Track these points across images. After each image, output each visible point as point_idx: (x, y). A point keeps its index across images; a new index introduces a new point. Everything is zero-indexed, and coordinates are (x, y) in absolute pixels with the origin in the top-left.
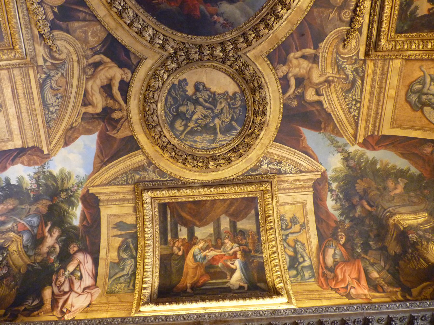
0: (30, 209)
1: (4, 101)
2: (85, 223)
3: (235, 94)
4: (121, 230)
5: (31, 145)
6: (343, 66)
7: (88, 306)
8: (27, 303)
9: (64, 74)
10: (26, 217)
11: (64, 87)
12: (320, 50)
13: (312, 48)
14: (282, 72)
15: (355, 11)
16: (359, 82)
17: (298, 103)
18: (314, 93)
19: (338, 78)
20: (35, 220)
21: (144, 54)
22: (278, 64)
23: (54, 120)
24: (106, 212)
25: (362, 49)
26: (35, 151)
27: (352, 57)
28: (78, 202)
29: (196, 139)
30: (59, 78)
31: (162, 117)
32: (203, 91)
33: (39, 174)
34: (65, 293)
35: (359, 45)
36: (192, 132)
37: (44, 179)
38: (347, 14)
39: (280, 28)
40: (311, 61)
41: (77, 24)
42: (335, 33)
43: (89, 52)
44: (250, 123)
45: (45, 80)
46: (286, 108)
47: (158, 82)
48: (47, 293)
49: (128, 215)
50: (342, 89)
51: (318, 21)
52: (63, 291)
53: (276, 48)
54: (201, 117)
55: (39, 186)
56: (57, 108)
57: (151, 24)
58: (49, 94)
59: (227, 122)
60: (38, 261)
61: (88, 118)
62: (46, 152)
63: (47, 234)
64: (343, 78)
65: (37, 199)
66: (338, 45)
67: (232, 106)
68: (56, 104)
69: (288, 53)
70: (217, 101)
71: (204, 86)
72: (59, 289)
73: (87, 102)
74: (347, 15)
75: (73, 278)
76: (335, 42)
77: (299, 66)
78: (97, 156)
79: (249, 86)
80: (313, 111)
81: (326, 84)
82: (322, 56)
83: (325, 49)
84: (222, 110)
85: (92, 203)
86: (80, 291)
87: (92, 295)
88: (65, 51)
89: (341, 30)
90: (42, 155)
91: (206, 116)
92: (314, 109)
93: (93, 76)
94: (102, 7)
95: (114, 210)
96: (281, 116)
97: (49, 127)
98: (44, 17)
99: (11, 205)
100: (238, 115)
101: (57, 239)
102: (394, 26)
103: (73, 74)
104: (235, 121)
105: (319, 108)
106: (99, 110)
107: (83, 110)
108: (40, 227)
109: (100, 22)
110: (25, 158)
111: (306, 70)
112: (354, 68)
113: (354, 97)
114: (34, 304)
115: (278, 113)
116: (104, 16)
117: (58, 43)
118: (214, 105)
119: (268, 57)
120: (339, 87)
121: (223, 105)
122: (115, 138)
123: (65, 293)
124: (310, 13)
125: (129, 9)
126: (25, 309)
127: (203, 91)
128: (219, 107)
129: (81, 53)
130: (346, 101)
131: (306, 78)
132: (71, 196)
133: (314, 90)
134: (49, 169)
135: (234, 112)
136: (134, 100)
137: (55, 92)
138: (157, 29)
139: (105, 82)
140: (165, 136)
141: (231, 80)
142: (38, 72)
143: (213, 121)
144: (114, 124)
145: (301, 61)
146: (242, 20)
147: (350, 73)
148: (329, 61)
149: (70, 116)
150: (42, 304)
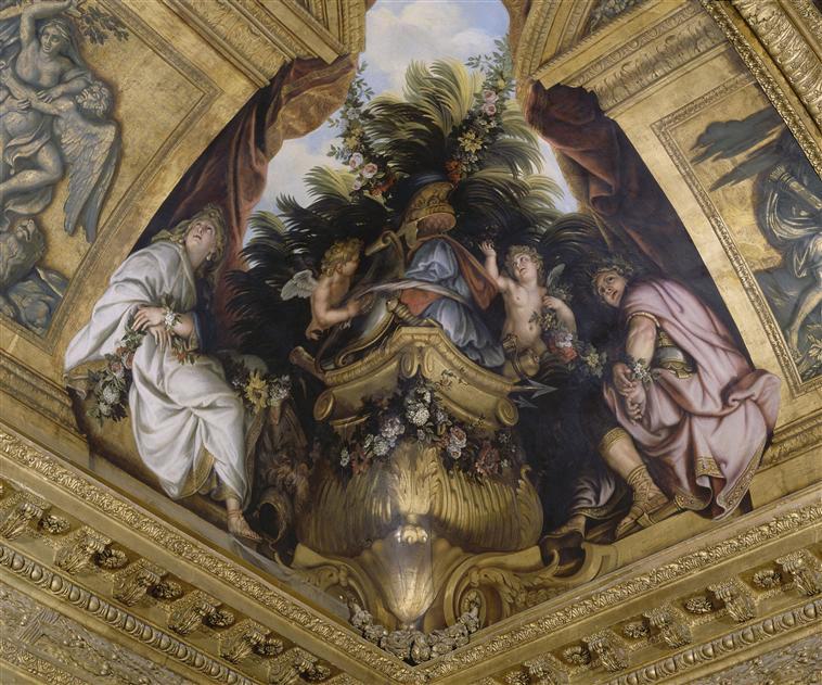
0: (403, 239)
2: (594, 192)
4: (730, 152)
5: (273, 70)
7: (769, 443)
8: (584, 504)
10: (408, 265)
20: (439, 260)
24: (639, 125)
26: (299, 74)
28: (531, 139)
34: (674, 431)
37: (382, 133)
48: (621, 452)
49: (726, 90)
52: (663, 427)
55: (382, 162)
60: (532, 373)
62: (329, 56)
63: (501, 283)
65: (403, 195)
72: (648, 427)
75: (670, 375)
85: (573, 115)
86: (713, 406)
87: (759, 405)
90: (326, 74)
95: (665, 98)
99: (344, 261)
101: (542, 283)
108: (468, 271)
110: (287, 114)
114: (603, 499)
123: (674, 431)
126: (591, 524)
132: (494, 132)
150: (625, 497)
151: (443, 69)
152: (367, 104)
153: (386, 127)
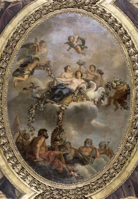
13: (135, 196)
21: (24, 191)
116: (3, 166)
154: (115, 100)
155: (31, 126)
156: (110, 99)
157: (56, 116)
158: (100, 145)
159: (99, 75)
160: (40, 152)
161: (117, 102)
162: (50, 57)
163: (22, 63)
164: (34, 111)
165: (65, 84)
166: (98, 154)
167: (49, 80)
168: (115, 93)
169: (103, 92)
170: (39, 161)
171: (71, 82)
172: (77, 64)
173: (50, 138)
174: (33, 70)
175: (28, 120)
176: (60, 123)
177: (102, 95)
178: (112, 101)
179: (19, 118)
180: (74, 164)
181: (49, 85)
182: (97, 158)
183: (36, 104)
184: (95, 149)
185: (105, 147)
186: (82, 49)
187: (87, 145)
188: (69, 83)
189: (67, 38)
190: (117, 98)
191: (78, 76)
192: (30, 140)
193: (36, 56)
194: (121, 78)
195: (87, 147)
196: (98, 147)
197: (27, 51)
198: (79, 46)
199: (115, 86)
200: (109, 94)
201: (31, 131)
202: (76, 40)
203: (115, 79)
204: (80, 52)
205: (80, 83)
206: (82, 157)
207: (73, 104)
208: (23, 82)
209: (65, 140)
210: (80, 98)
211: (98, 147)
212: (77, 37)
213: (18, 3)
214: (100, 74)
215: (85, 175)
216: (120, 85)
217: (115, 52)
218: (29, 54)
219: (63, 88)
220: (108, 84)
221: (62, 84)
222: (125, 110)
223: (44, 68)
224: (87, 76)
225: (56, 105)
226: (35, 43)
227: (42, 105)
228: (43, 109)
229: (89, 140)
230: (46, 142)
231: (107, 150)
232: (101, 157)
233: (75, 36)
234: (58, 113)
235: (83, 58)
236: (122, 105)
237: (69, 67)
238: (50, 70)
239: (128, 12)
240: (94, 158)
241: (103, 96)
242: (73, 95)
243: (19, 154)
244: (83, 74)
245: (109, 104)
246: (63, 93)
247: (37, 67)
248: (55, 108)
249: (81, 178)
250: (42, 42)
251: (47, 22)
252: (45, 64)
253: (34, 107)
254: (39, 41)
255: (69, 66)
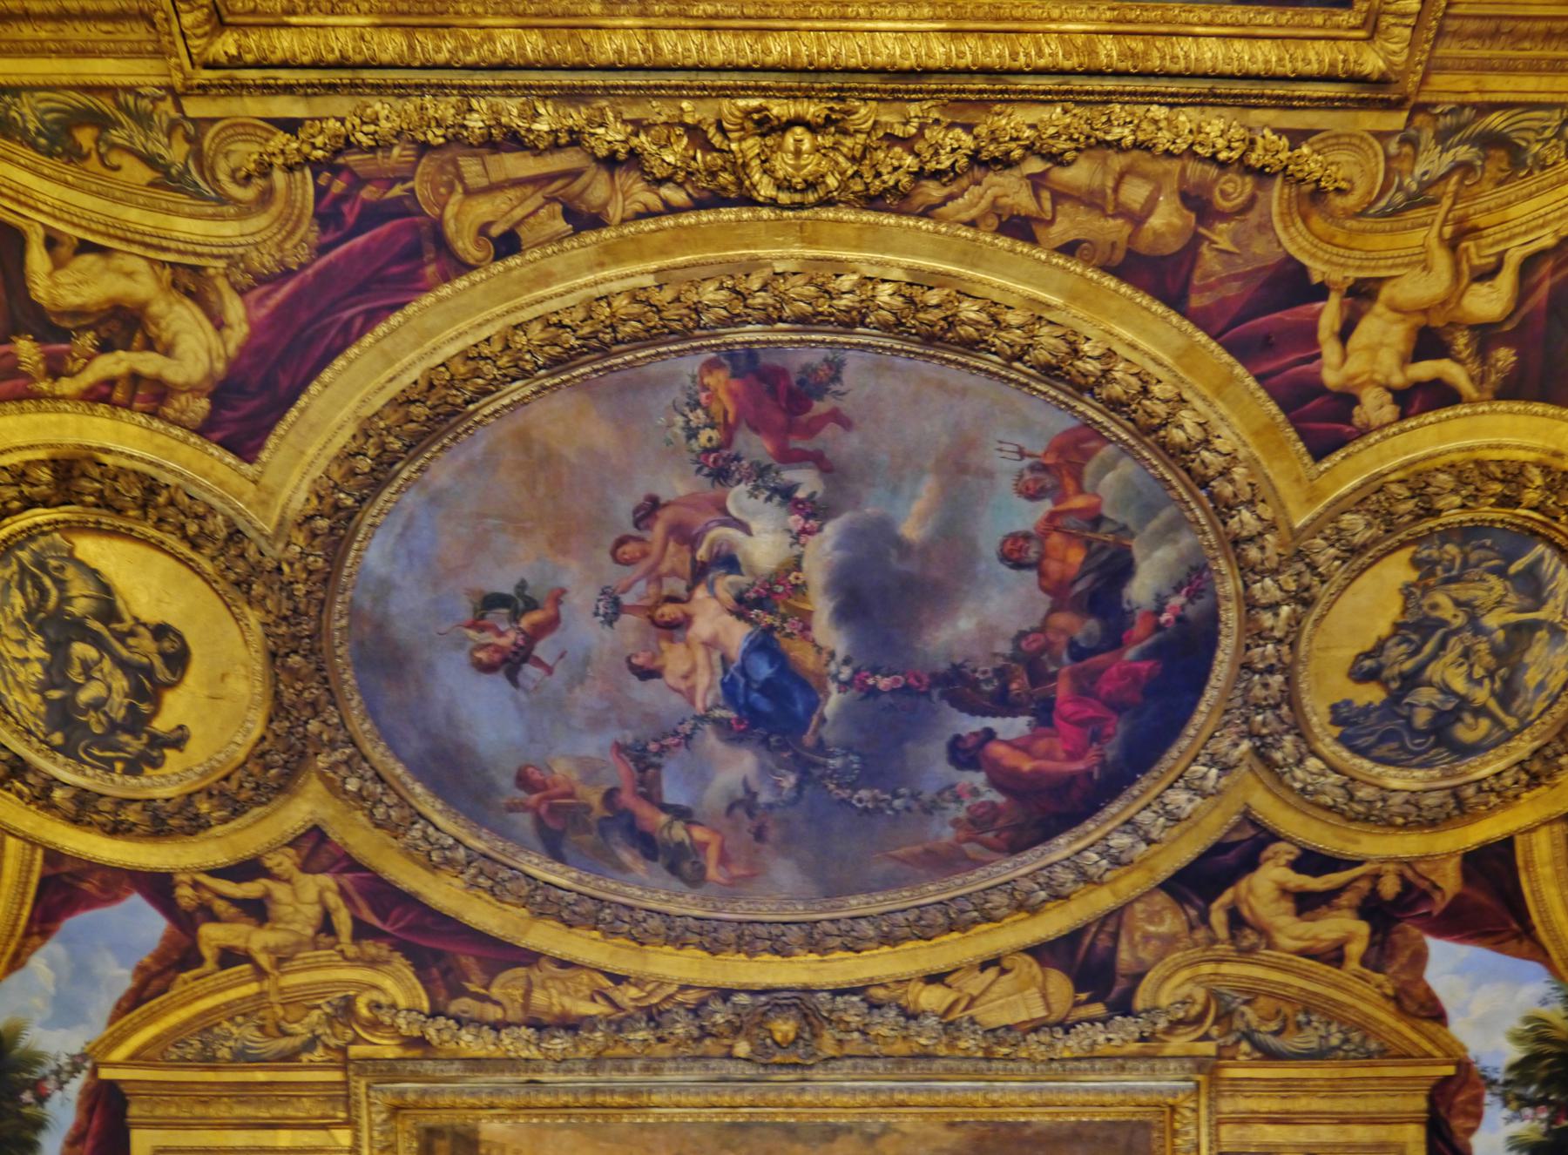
1: (1297, 1146)
3: (1415, 563)
6: (1414, 187)
9: (1246, 997)
11: (1281, 1003)
12: (1336, 276)
13: (1319, 305)
14: (1381, 407)
15: (1224, 165)
16: (1496, 121)
17: (1508, 345)
18: (1481, 289)
19: (1454, 203)
21: (1235, 809)
22: (1350, 424)
23: (1365, 1038)
25: (1371, 120)
27: (1388, 158)
29: (1532, 684)
30: (1256, 1010)
31: (1433, 779)
32: (1383, 660)
33: (1510, 1096)
35: (1350, 136)
36: (1506, 696)
37: (1527, 1085)
38: (1229, 188)
39: (1234, 420)
40: (1365, 306)
41: (1124, 956)
42: (1286, 228)
43: (1200, 934)
44: (1531, 519)
45: (1256, 1046)
46: (1511, 390)
47: (1328, 788)
50: (1500, 183)
51: (1233, 289)
53: (1298, 431)
54: (1465, 668)
55: (1544, 1101)
56: (1334, 1028)
57: (1156, 791)
58: (1293, 1042)
59: (1506, 589)
61: (1378, 956)
62: (1450, 1070)
64: (1461, 182)
66: (1330, 216)
67: (1454, 573)
68: (1322, 1028)
69: (1320, 389)
70: (1426, 617)
71: (1367, 655)
73: (1333, 955)
74: (1236, 189)
76: (1318, 223)
77: (1373, 349)
78: (1498, 946)
79: (1406, 524)
80: (1552, 288)
81: (1464, 245)
82: (1359, 268)
83: (1335, 259)
84: (1458, 603)
88: (1186, 989)
89: (1280, 204)
91: (1466, 654)
92: (1547, 284)
93: (1264, 932)
94: (1092, 897)
96: (1539, 408)
97: (1384, 1053)
98: (1099, 1025)
100: (1490, 554)
102: (1319, 20)
103: (1249, 978)
104: (1510, 563)
105: (1547, 266)
106: (1363, 928)
107: (1353, 965)
109: (1129, 904)
110: (1458, 1123)
111: (1396, 322)
112: (1432, 144)
113: (1548, 134)
115: (1522, 421)
116: (1114, 893)
117: (1164, 1000)
118: (1434, 629)
119: (1318, 454)
120: (1490, 197)
121: (1441, 598)
122: (1458, 898)
124: (1201, 320)
125: (1111, 843)
127: (1383, 660)
128: (1447, 610)
129: (1196, 953)
130: (1555, 163)
131: (1420, 320)
133: (1476, 287)
134: (1502, 1069)
135: (1477, 566)
136: (1357, 842)
137: (1291, 1027)
138: (1172, 777)
139: (1288, 905)
140: (1498, 775)
141: (1368, 574)
142: (1233, 1058)
143: (1488, 633)
144: (1414, 893)
145: (1359, 338)
146: (1186, 540)
147: (1448, 158)
148: (1380, 242)
149: (1363, 999)
151: (1528, 1020)
152: (1501, 1077)
153: (1525, 1080)
154: (790, 429)
155: (933, 801)
156: (789, 457)
157: (886, 699)
158: (1033, 495)
159: (666, 516)
160: (1056, 761)
161: (804, 418)
162: (594, 746)
163: (636, 852)
164: (864, 793)
165: (725, 671)
166: (1078, 502)
167: (710, 740)
168: (756, 430)
169: (752, 495)
170: (1096, 760)
171: (710, 644)
172: (616, 624)
173: (990, 722)
174: (665, 808)
175: (904, 813)
176: (919, 681)
177: (769, 499)
178: (797, 443)
179: (898, 848)
180: (1123, 612)
181: (733, 735)
182: (1097, 507)
183: (832, 786)
184: (1052, 516)
185: (1045, 468)
186: (532, 605)
187: (1032, 554)
188: (716, 656)
189: (485, 677)
190: (780, 419)
191: (680, 615)
192: (998, 798)
193: (595, 799)
194: (669, 402)
195: (1043, 556)
196: (1046, 506)
197: (575, 838)
198: (517, 621)
199: (715, 434)
200: (758, 464)
201: (958, 799)
202: (488, 637)
203: (675, 435)
204: (551, 612)
205: (713, 605)
206: (1090, 578)
207: (829, 634)
208: (727, 843)
209: (1003, 656)
210: (791, 601)
211: (1046, 506)
212: (472, 633)
213: (350, 888)
214: (659, 513)
215: (1182, 560)
216: (706, 410)
217: (523, 439)
218: (588, 830)
219: (742, 681)
220: (706, 470)
221: (723, 684)
222: (848, 375)
223: (652, 766)
224: (673, 573)
225: (833, 702)
226: (535, 810)
227: (836, 763)
228: (852, 757)
229: (1008, 546)
230: (1012, 736)
231: (1061, 461)
232: (1095, 485)
233: (470, 645)
234: (873, 692)
235: (581, 600)
236: (820, 391)
237: (634, 661)
238: (655, 741)
239: (284, 381)
240: (1097, 520)
241: (775, 491)
242: (776, 635)
243: (1062, 840)
244: (665, 592)
245: (818, 461)
246: (768, 681)
247: (651, 796)
248: (845, 711)
249: (1199, 577)
250: (523, 780)
251: (419, 770)
252: (631, 764)
253: (845, 794)
254: (521, 795)
255: (629, 660)
